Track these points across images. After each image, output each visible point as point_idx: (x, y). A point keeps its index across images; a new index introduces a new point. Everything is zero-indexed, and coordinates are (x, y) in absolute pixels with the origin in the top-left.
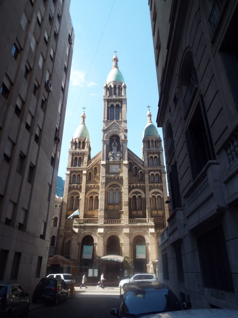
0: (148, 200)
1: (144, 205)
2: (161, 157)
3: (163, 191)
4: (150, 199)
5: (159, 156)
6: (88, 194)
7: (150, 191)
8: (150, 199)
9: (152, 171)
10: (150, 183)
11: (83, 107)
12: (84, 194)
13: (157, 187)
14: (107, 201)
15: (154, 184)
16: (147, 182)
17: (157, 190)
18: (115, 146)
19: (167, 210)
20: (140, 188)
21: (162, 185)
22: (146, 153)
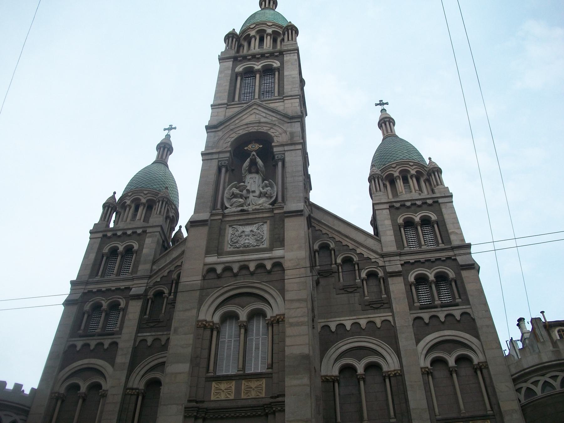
2: (446, 216)
4: (426, 373)
5: (440, 213)
7: (418, 341)
8: (426, 373)
10: (411, 307)
11: (167, 127)
12: (125, 372)
14: (204, 363)
15: (433, 312)
17: (448, 334)
18: (253, 168)
21: (468, 311)
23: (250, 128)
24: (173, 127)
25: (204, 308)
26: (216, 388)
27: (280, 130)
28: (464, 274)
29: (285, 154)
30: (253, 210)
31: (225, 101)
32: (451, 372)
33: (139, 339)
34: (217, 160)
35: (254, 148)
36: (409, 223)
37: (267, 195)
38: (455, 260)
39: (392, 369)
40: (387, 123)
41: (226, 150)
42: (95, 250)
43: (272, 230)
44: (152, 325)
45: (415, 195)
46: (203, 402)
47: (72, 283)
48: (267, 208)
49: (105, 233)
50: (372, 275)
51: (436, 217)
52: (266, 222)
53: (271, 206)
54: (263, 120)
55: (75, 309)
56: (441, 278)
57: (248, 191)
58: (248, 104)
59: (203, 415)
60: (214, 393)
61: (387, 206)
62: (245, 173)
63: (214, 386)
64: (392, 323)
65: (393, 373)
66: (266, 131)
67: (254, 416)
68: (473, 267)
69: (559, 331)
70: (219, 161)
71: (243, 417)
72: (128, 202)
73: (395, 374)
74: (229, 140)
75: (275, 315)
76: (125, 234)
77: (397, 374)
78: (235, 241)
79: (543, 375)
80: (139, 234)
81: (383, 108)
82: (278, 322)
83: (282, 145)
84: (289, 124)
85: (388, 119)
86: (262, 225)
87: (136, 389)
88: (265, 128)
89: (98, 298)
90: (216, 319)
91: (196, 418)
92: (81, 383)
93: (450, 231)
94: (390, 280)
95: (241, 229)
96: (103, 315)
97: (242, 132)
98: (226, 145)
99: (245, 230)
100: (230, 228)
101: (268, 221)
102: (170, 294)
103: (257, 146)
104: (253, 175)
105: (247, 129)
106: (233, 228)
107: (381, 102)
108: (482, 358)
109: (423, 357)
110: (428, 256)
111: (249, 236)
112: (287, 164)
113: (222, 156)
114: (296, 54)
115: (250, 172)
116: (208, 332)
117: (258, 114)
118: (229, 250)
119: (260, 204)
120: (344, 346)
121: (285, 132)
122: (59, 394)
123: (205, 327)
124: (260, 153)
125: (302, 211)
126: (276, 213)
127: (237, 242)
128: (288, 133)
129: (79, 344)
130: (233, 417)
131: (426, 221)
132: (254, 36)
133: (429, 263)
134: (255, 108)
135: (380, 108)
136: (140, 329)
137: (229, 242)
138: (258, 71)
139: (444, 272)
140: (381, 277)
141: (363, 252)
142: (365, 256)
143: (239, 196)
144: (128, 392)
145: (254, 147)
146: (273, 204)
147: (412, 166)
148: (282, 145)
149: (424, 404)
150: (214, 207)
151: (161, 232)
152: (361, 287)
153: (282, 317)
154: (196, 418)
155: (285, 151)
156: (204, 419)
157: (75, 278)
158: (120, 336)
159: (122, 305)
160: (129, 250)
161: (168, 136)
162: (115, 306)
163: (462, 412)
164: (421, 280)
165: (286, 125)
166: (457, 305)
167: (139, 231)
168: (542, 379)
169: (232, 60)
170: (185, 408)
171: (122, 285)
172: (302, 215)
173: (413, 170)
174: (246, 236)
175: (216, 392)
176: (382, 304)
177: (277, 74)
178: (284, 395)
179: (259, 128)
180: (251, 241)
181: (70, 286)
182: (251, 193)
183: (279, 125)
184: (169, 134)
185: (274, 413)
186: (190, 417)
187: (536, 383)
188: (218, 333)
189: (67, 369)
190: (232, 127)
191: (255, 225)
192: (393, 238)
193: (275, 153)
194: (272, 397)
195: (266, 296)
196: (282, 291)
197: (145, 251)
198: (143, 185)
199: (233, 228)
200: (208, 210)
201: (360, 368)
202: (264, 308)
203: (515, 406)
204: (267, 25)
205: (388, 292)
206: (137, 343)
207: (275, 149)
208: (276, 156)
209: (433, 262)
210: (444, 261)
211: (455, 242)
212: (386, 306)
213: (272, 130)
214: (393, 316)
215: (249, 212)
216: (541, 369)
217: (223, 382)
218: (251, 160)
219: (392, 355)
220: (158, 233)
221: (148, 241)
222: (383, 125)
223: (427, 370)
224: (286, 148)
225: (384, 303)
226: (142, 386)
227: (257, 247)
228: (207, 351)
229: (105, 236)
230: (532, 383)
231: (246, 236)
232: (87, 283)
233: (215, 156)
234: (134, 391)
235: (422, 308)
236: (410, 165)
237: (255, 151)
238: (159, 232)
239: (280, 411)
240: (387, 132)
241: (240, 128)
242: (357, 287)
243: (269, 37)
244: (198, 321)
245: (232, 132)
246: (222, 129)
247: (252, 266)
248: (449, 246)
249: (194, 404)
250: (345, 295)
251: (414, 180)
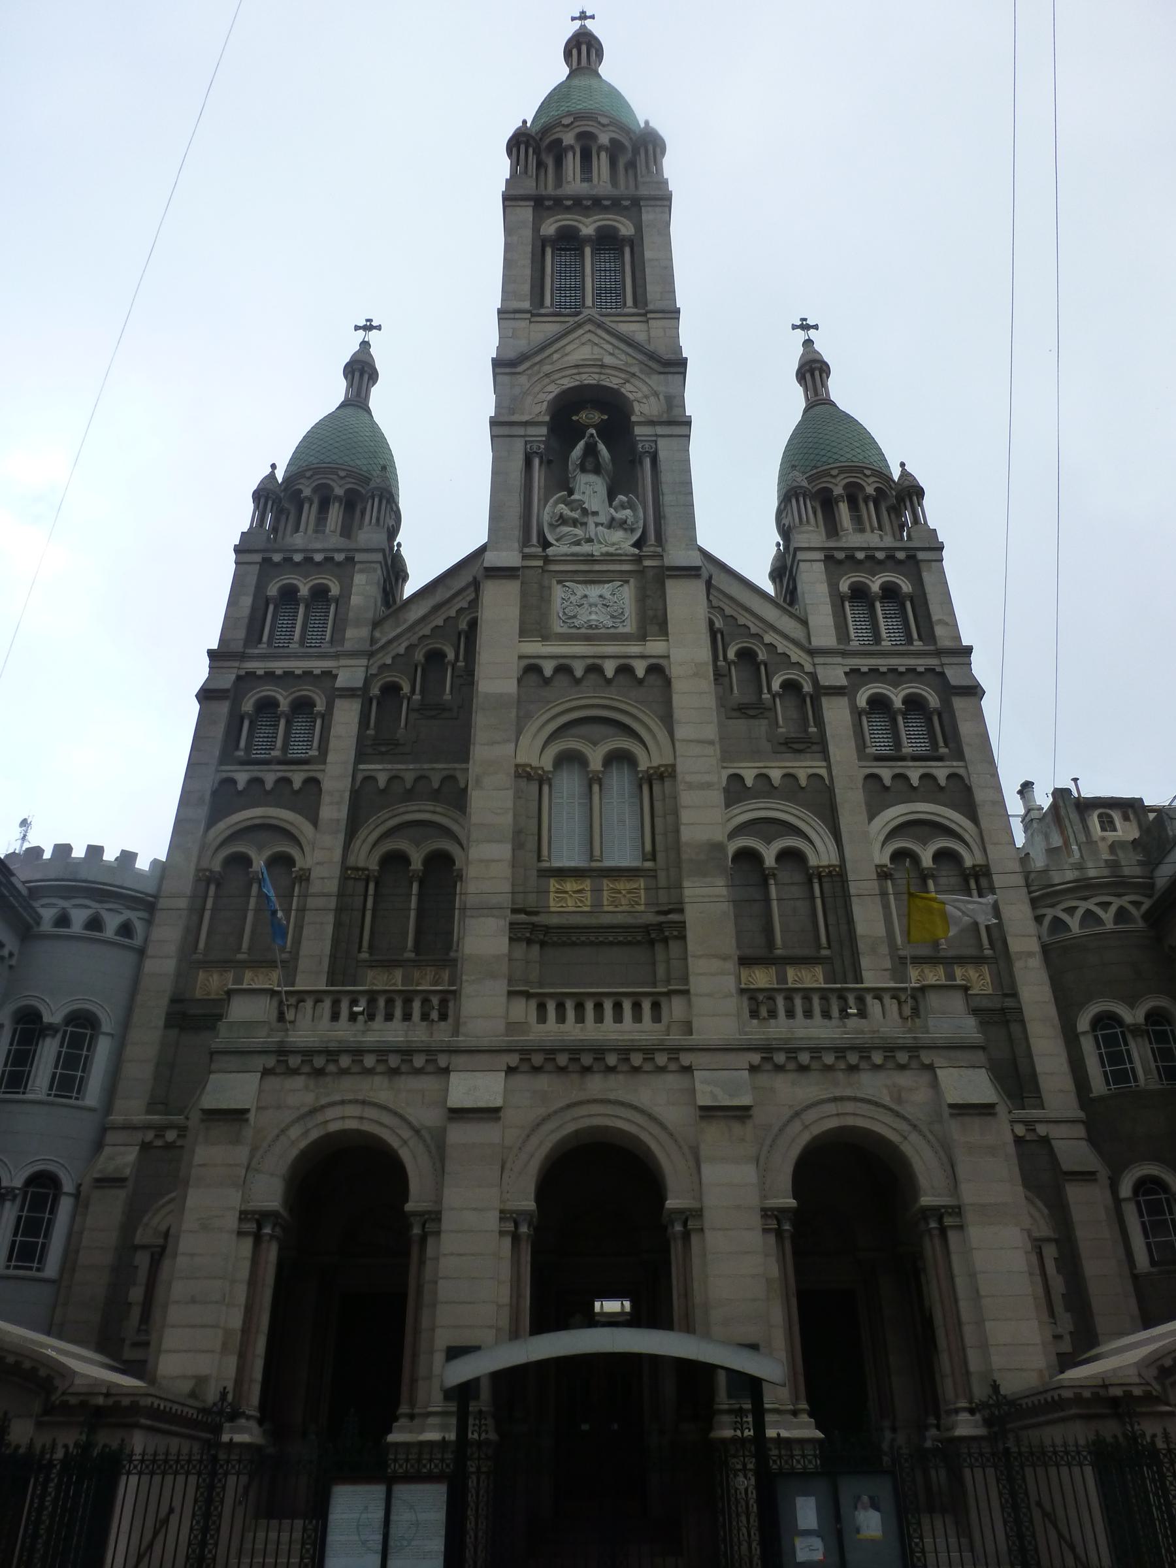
0: (861, 881)
1: (831, 920)
2: (928, 589)
3: (975, 819)
4: (883, 874)
5: (919, 583)
6: (368, 834)
7: (871, 818)
8: (883, 874)
9: (875, 674)
11: (362, 323)
12: (341, 837)
13: (930, 788)
14: (532, 844)
15: (899, 767)
16: (842, 749)
17: (924, 809)
18: (590, 462)
19: (1030, 954)
20: (791, 789)
21: (961, 771)
22: (820, 567)
23: (584, 376)
24: (374, 324)
25: (525, 740)
26: (558, 889)
27: (645, 389)
28: (958, 703)
29: (658, 443)
30: (602, 555)
31: (526, 305)
32: (924, 877)
33: (360, 777)
34: (522, 440)
35: (592, 419)
36: (859, 594)
37: (625, 526)
38: (942, 674)
39: (825, 863)
40: (817, 373)
41: (541, 419)
42: (251, 589)
43: (642, 599)
44: (383, 749)
45: (872, 539)
46: (536, 913)
48: (629, 553)
49: (267, 555)
50: (790, 686)
51: (910, 587)
52: (627, 582)
53: (637, 551)
54: (608, 360)
55: (223, 708)
56: (914, 704)
57: (585, 512)
58: (577, 319)
59: (541, 937)
60: (554, 899)
61: (820, 555)
62: (575, 470)
63: (554, 886)
64: (827, 782)
65: (827, 870)
66: (616, 387)
67: (629, 943)
68: (974, 691)
69: (1100, 816)
70: (526, 442)
71: (611, 944)
72: (307, 492)
73: (830, 872)
74: (542, 396)
75: (655, 764)
76: (309, 560)
77: (834, 873)
78: (572, 614)
79: (1085, 899)
80: (339, 564)
81: (807, 338)
82: (661, 777)
83: (651, 423)
84: (662, 377)
85: (818, 365)
86: (621, 586)
87: (364, 869)
88: (615, 381)
89: (268, 690)
90: (547, 762)
91: (529, 942)
92: (252, 854)
93: (935, 618)
94: (825, 701)
95: (581, 590)
96: (282, 722)
97: (568, 383)
98: (537, 407)
99: (587, 593)
100: (559, 586)
101: (632, 580)
102: (413, 691)
103: (596, 417)
104: (592, 478)
105: (577, 377)
106: (565, 586)
107: (804, 323)
108: (979, 859)
109: (879, 845)
110: (894, 661)
111: (596, 606)
112: (663, 465)
113: (532, 431)
114: (667, 209)
115: (583, 469)
116: (534, 787)
117: (596, 344)
118: (560, 630)
119: (614, 544)
121: (656, 394)
122: (211, 871)
123: (529, 777)
124: (605, 431)
125: (698, 568)
126: (647, 567)
127: (575, 617)
128: (661, 397)
129: (242, 778)
130: (592, 944)
131: (890, 592)
132: (572, 147)
133: (895, 676)
134: (589, 331)
135: (801, 335)
136: (361, 756)
137: (561, 616)
138: (588, 240)
139: (920, 695)
140: (808, 693)
141: (775, 643)
142: (780, 651)
143: (571, 521)
144: (349, 874)
145: (590, 417)
146: (638, 544)
147: (867, 476)
148: (651, 423)
149: (880, 930)
150: (526, 541)
151: (383, 563)
152: (771, 709)
153: (670, 770)
155: (656, 435)
156: (543, 944)
158: (321, 767)
159: (320, 707)
160: (320, 594)
161: (365, 345)
162: (302, 706)
163: (941, 947)
164: (879, 704)
165: (655, 377)
166: (940, 759)
167: (339, 557)
168: (1083, 906)
169: (532, 203)
170: (511, 924)
171: (317, 666)
172: (698, 576)
173: (869, 485)
174: (591, 605)
175: (558, 897)
176: (810, 745)
177: (627, 250)
178: (681, 911)
179: (603, 377)
180: (598, 617)
181: (207, 661)
182: (590, 517)
183: (643, 376)
184: (366, 339)
185: (665, 941)
187: (1071, 911)
188: (550, 786)
189: (222, 825)
190: (547, 368)
191: (606, 586)
192: (830, 621)
193: (638, 438)
194: (659, 913)
195: (635, 726)
196: (668, 719)
197: (355, 600)
198: (334, 457)
199: (565, 586)
200: (516, 545)
201: (769, 856)
202: (633, 749)
203: (1034, 946)
205: (820, 722)
206: (358, 784)
207: (638, 430)
208: (640, 446)
209: (902, 673)
210: (921, 673)
211: (945, 643)
212: (815, 748)
214: (829, 768)
215: (594, 558)
216: (1083, 888)
217: (568, 879)
218: (587, 445)
219: (827, 840)
220: (378, 566)
221: (359, 579)
222: (808, 376)
223: (885, 869)
224: (660, 430)
225: (813, 743)
226: (374, 866)
227: (612, 631)
228: (535, 821)
229: (267, 561)
230: (1064, 910)
231: (591, 605)
232: (243, 657)
233: (520, 431)
234: (360, 873)
235: (879, 758)
236: (865, 475)
237: (594, 426)
238: (380, 563)
239: (676, 938)
240: (816, 394)
241: (563, 374)
242: (764, 709)
243: (603, 155)
244: (517, 766)
245: (547, 380)
246: (528, 369)
247: (610, 668)
248: (932, 648)
249: (522, 917)
251: (871, 505)
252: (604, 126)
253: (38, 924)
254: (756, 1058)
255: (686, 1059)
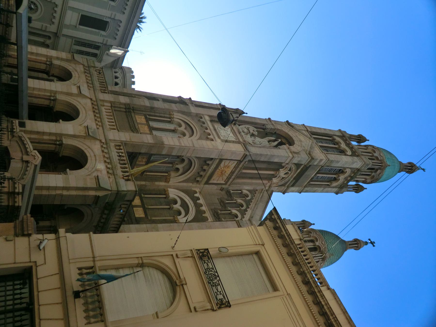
47: (190, 98)
71: (129, 124)
120: (187, 199)
138: (340, 146)
154: (125, 108)
156: (126, 112)
157: (193, 99)
181: (188, 98)
186: (125, 106)
204: (380, 154)
213: (297, 146)
240: (350, 245)
250: (218, 202)
252: (380, 155)
253: (114, 69)
254: (103, 141)
255: (101, 128)
